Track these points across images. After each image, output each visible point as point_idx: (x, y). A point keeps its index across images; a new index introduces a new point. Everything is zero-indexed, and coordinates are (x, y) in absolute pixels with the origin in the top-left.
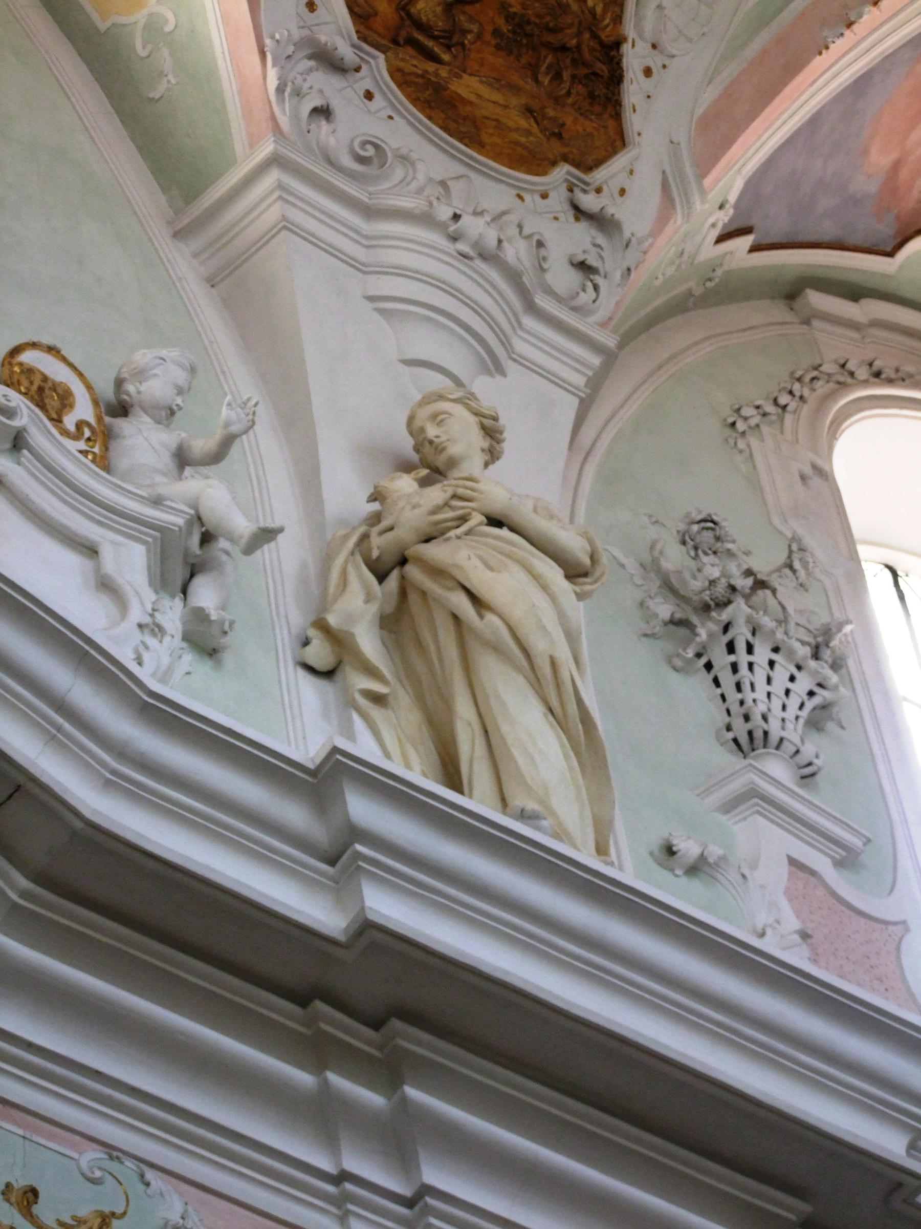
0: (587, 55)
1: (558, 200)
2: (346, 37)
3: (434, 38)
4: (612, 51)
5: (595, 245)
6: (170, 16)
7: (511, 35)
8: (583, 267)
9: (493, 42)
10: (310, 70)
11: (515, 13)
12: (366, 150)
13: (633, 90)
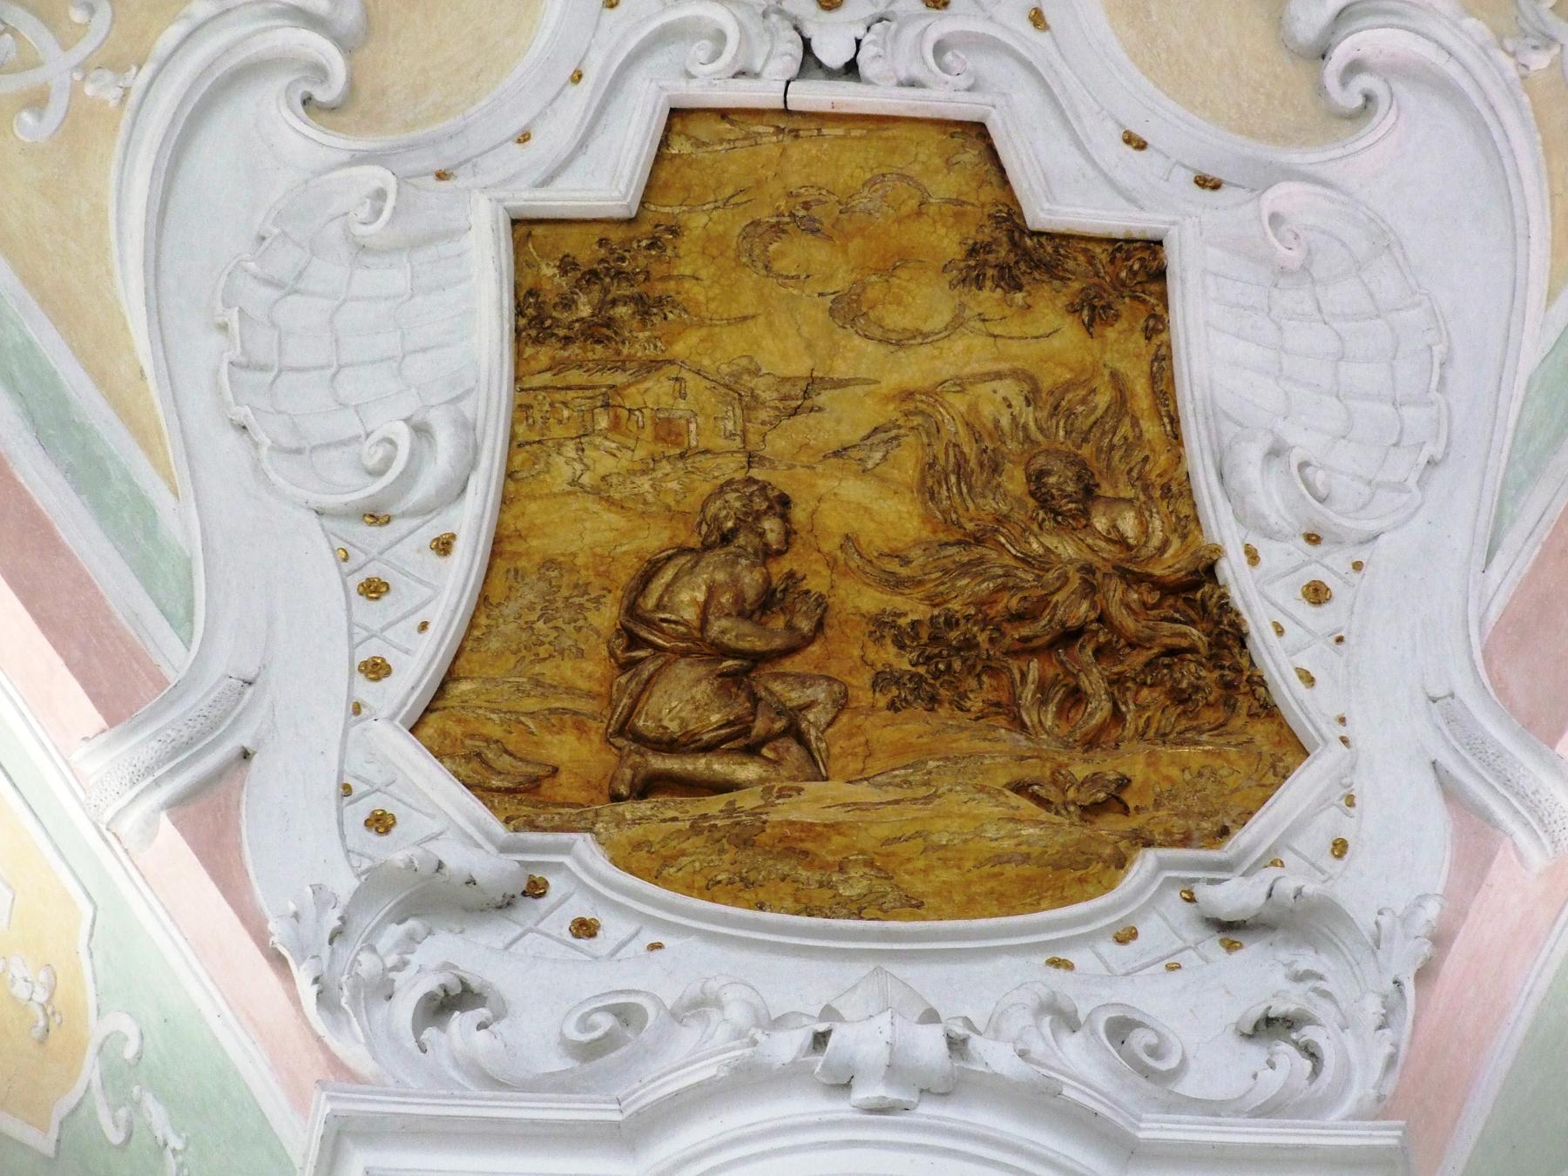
0: (1130, 624)
1: (1167, 926)
2: (478, 837)
3: (709, 748)
4: (1197, 590)
5: (1299, 978)
6: (129, 1027)
7: (922, 670)
8: (1271, 1026)
9: (882, 701)
11: (914, 624)
12: (593, 1028)
13: (1283, 642)
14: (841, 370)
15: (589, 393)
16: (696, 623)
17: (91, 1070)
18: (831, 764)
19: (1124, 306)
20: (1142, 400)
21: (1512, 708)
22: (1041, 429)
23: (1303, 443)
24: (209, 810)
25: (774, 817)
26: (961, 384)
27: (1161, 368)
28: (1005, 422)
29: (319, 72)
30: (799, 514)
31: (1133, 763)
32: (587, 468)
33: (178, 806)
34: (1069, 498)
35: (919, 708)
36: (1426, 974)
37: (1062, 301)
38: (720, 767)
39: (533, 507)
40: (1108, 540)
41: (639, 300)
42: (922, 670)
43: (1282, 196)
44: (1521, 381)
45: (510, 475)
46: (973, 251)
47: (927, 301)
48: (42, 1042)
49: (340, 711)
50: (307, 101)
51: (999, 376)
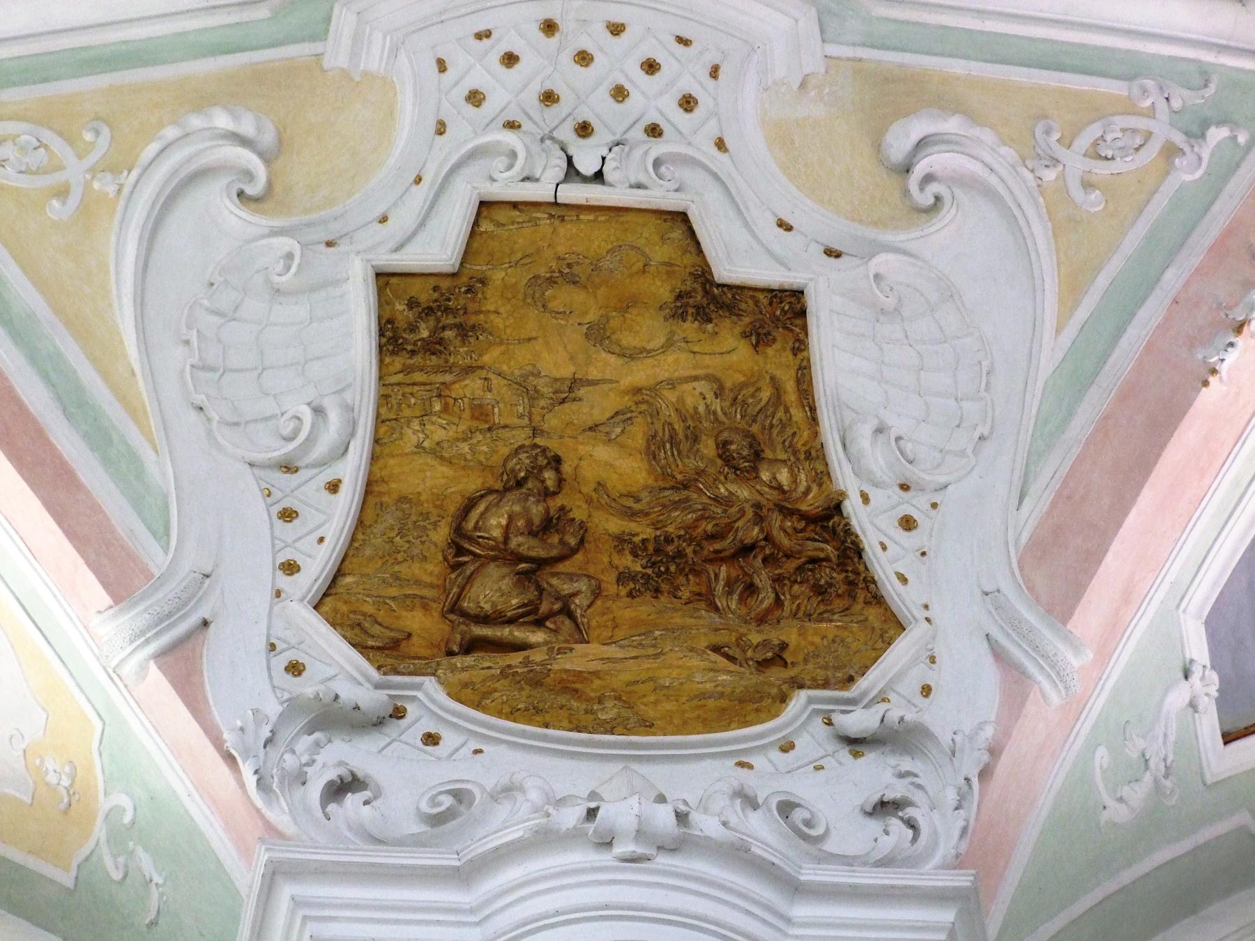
0: (785, 542)
1: (813, 741)
2: (361, 679)
3: (511, 621)
5: (902, 775)
7: (649, 571)
8: (884, 807)
9: (624, 592)
10: (317, 744)
11: (644, 541)
12: (439, 804)
13: (887, 555)
14: (594, 374)
15: (428, 387)
16: (501, 539)
17: (99, 831)
18: (591, 632)
19: (779, 333)
20: (791, 396)
21: (1038, 600)
22: (725, 414)
23: (898, 426)
24: (182, 659)
25: (556, 667)
26: (672, 384)
27: (803, 374)
28: (701, 409)
29: (249, 175)
30: (567, 468)
31: (789, 633)
32: (427, 436)
33: (161, 656)
34: (744, 459)
35: (648, 596)
36: (985, 774)
37: (738, 330)
38: (518, 634)
39: (392, 462)
40: (771, 487)
41: (459, 327)
42: (649, 571)
43: (883, 262)
44: (1040, 384)
45: (377, 441)
46: (679, 297)
47: (648, 329)
48: (66, 812)
49: (268, 594)
50: (241, 194)
51: (696, 378)
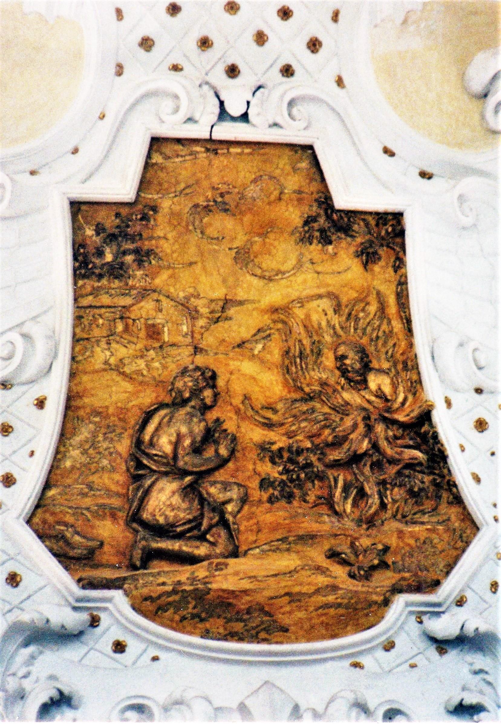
0: (389, 451)
1: (409, 641)
3: (180, 536)
4: (421, 429)
7: (284, 477)
9: (265, 496)
10: (33, 657)
11: (281, 450)
14: (241, 295)
15: (113, 310)
16: (171, 455)
18: (240, 537)
19: (382, 252)
22: (342, 328)
25: (214, 586)
26: (302, 302)
27: (402, 290)
28: (324, 324)
30: (221, 383)
32: (112, 355)
35: (283, 503)
37: (352, 249)
39: (85, 378)
40: (377, 396)
41: (137, 251)
42: (284, 477)
45: (73, 358)
46: (306, 223)
47: (284, 252)
51: (320, 296)
